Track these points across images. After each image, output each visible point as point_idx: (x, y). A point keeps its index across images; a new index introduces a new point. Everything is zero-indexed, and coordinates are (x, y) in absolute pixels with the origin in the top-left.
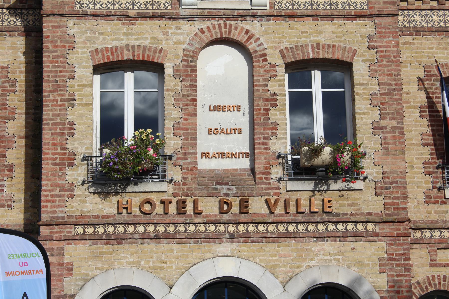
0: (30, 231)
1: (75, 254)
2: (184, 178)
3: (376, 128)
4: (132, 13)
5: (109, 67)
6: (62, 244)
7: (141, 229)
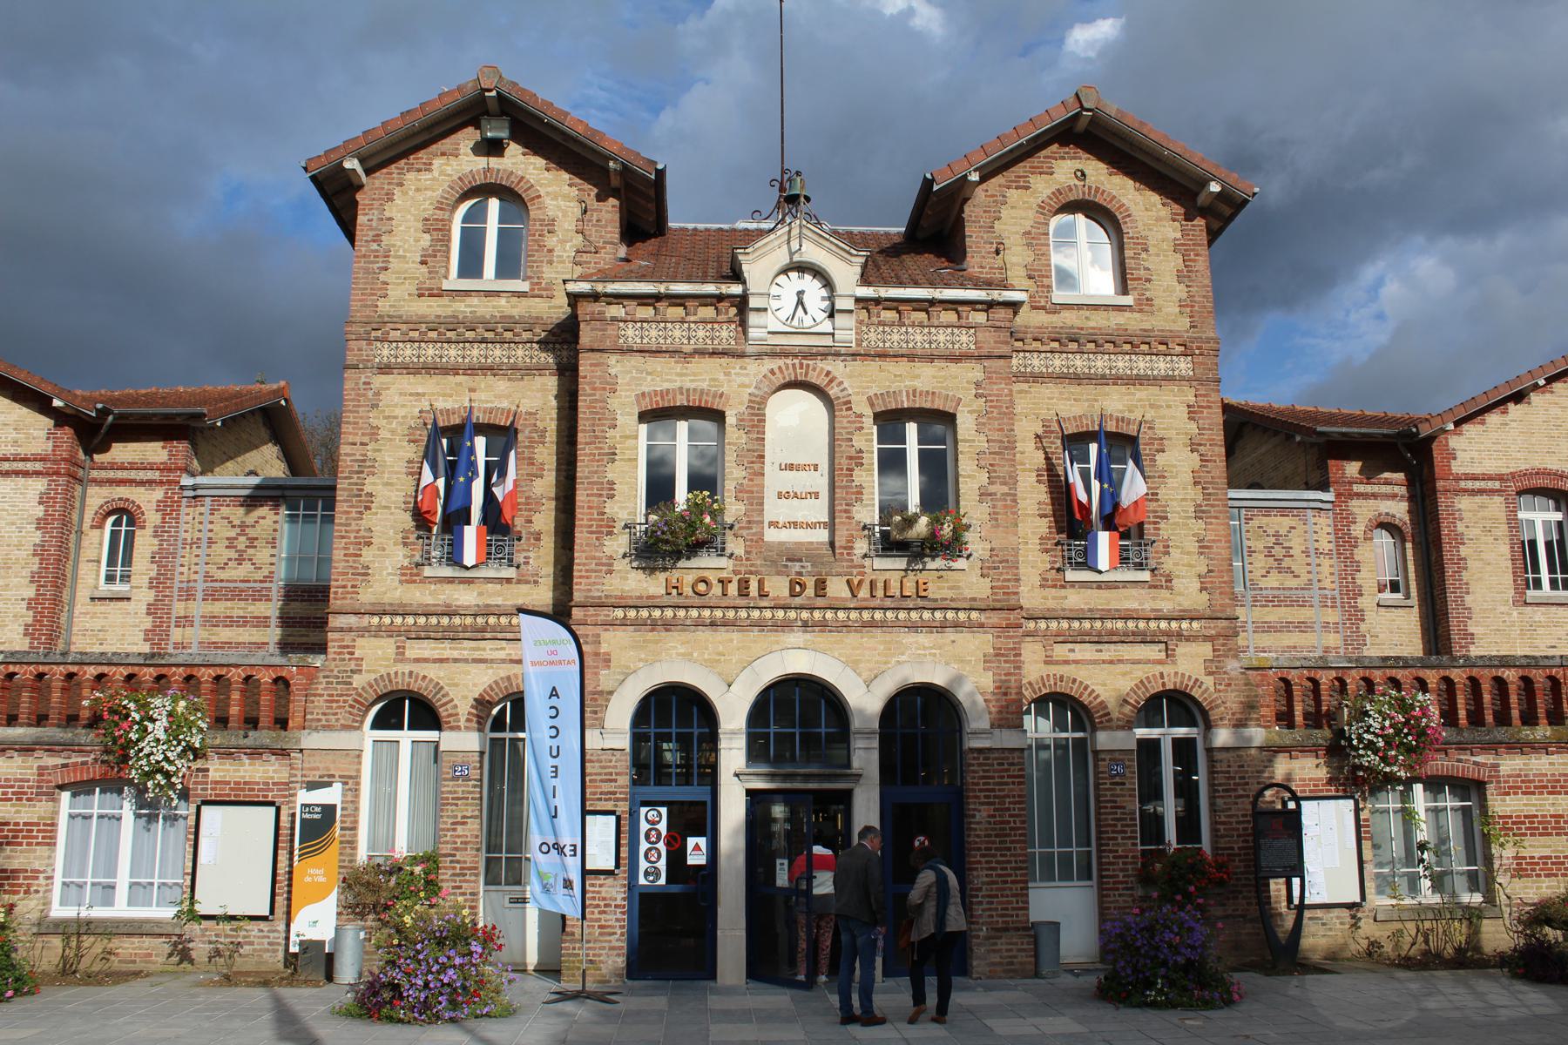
0: (561, 613)
1: (614, 642)
2: (747, 552)
3: (984, 494)
4: (688, 349)
5: (658, 415)
6: (598, 630)
7: (694, 613)
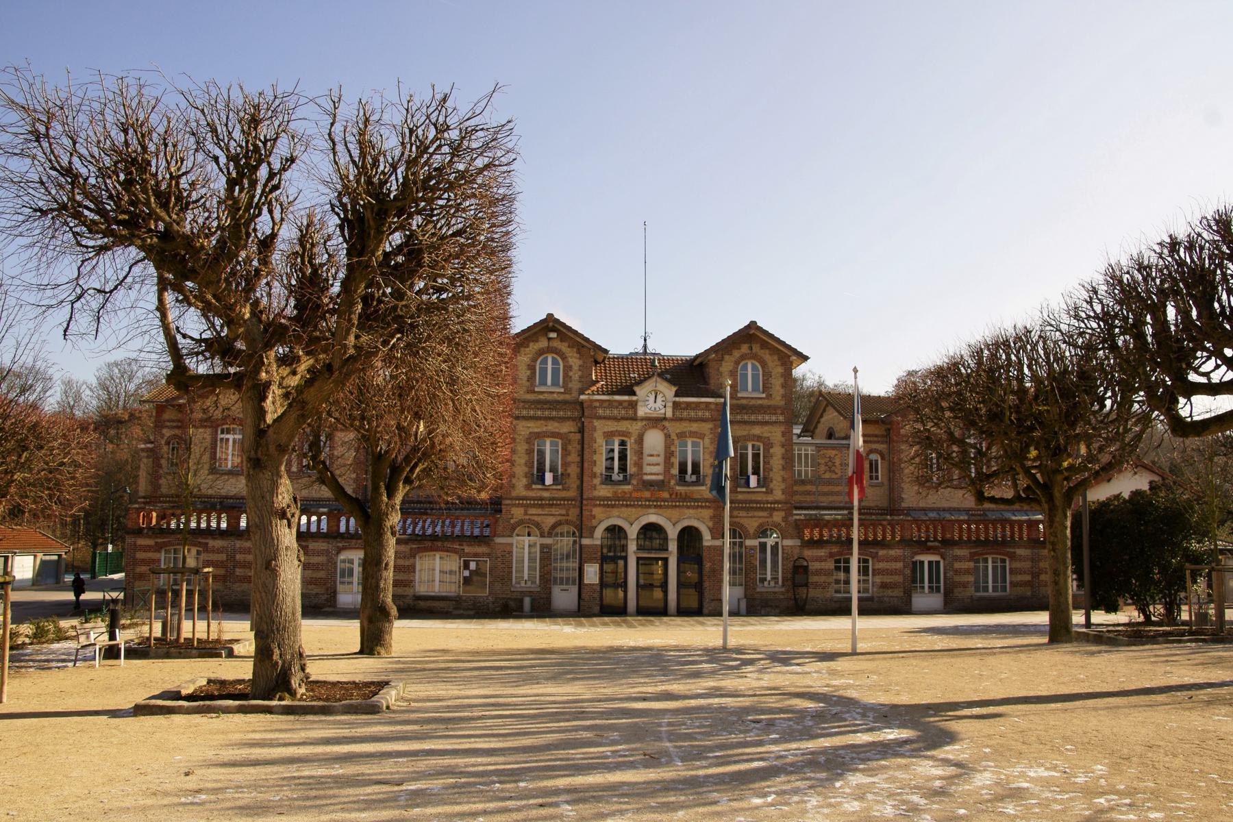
5: (609, 435)
